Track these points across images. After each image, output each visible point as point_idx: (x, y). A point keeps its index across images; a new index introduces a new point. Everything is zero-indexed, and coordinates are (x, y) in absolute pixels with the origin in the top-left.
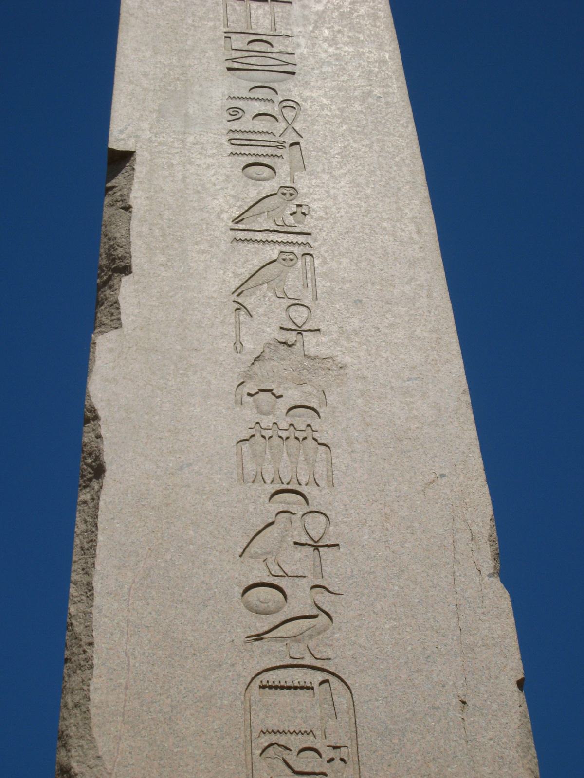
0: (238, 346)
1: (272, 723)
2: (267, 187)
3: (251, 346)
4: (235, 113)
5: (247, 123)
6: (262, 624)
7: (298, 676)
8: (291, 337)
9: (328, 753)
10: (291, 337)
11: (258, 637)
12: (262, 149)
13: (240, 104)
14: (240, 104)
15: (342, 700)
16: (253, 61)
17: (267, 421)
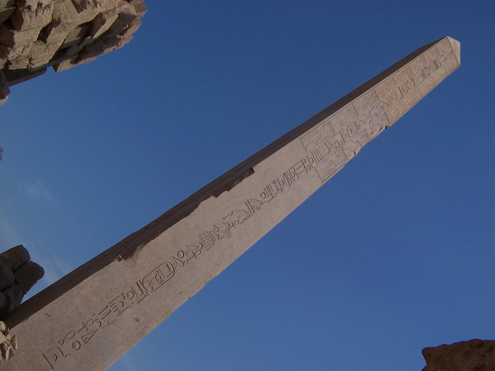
0: (224, 219)
1: (161, 269)
2: (261, 200)
3: (225, 221)
4: (274, 182)
5: (273, 186)
6: (176, 257)
7: (171, 268)
8: (231, 225)
9: (161, 280)
10: (231, 225)
11: (174, 258)
12: (267, 192)
13: (277, 182)
14: (277, 182)
15: (171, 276)
16: (289, 176)
17: (213, 233)
